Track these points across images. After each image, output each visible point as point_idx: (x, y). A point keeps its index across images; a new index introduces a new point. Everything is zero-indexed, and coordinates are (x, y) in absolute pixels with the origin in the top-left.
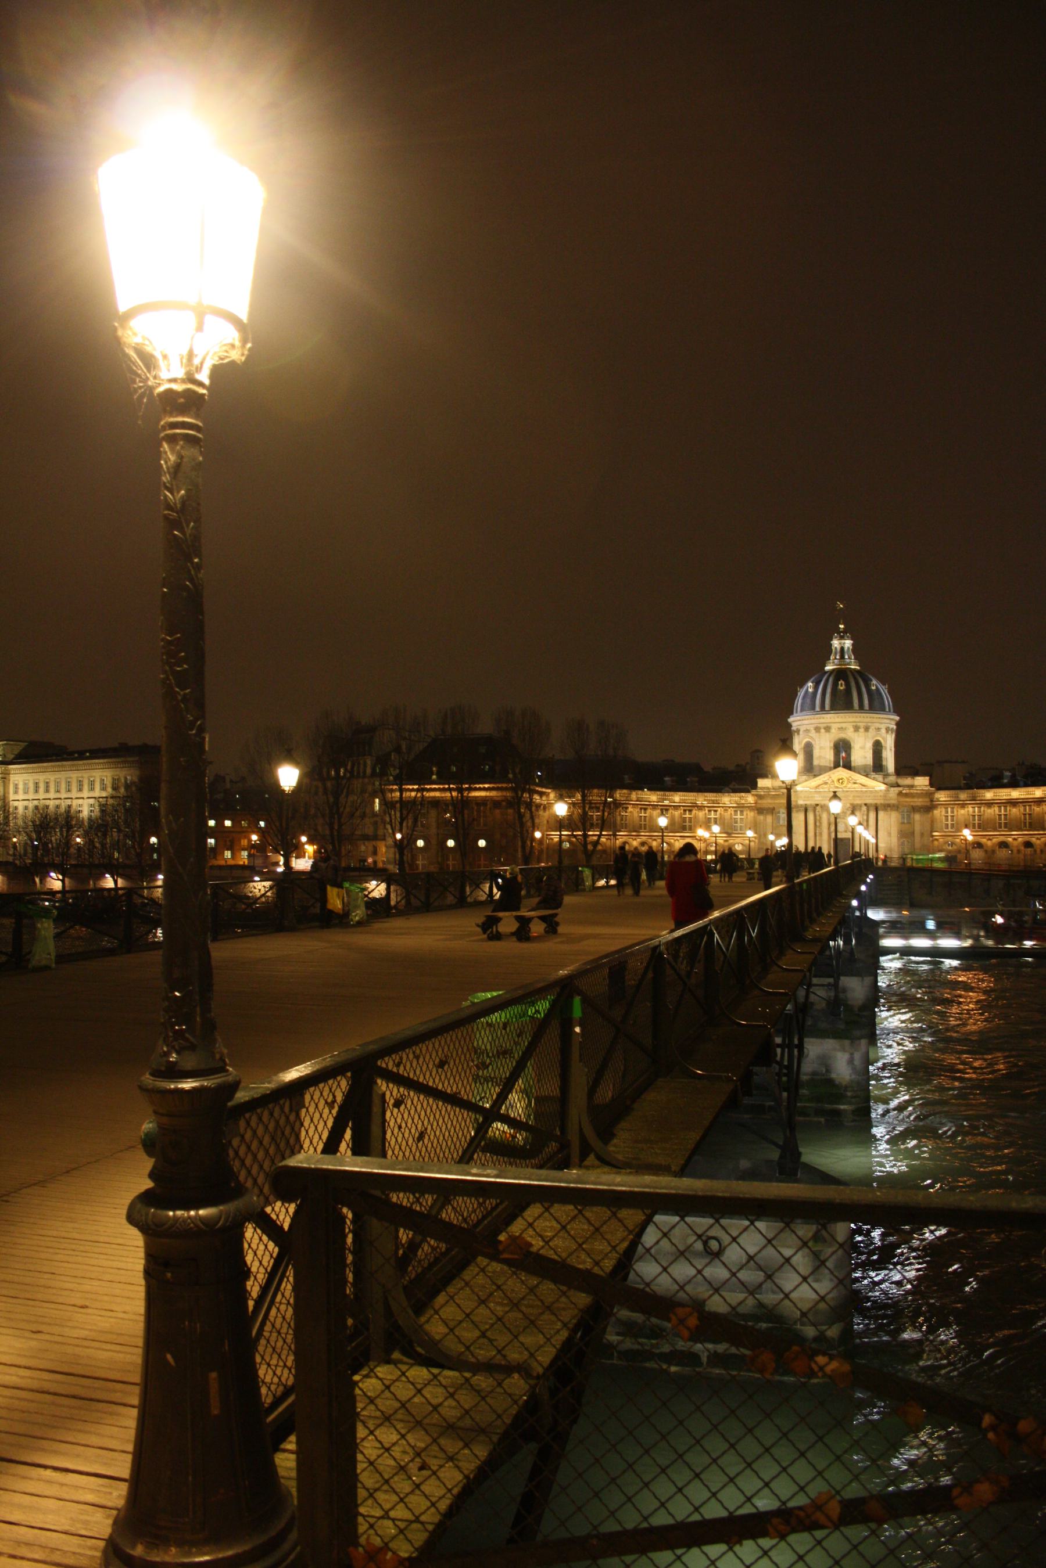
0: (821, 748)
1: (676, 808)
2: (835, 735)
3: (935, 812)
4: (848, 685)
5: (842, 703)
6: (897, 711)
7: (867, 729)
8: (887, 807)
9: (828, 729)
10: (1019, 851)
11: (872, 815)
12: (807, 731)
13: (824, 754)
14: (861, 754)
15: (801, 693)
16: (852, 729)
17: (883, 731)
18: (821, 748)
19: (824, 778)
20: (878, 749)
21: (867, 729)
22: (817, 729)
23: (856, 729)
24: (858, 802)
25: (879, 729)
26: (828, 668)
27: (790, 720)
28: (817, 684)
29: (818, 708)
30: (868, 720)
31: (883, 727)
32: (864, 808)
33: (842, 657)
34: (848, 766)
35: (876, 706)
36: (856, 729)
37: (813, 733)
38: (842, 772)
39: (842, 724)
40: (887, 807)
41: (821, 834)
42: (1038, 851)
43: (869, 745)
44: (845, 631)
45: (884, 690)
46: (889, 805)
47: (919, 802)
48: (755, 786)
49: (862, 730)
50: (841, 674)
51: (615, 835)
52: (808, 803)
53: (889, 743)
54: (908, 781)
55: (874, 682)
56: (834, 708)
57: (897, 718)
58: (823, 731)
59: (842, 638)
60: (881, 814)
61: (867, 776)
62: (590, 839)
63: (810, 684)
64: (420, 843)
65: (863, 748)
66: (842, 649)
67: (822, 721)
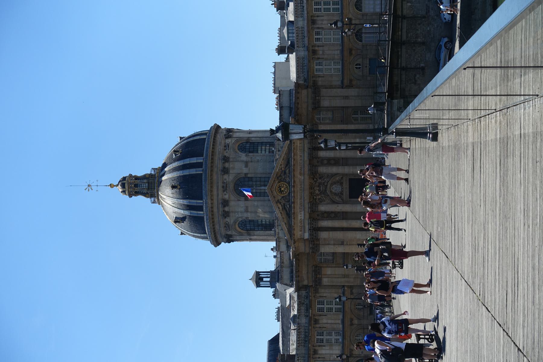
0: (247, 211)
3: (320, 83)
7: (226, 159)
9: (225, 203)
16: (226, 176)
17: (228, 141)
18: (247, 211)
22: (226, 214)
23: (225, 171)
25: (226, 146)
30: (216, 158)
36: (225, 171)
37: (230, 220)
43: (243, 157)
52: (307, 227)
58: (226, 209)
65: (246, 164)
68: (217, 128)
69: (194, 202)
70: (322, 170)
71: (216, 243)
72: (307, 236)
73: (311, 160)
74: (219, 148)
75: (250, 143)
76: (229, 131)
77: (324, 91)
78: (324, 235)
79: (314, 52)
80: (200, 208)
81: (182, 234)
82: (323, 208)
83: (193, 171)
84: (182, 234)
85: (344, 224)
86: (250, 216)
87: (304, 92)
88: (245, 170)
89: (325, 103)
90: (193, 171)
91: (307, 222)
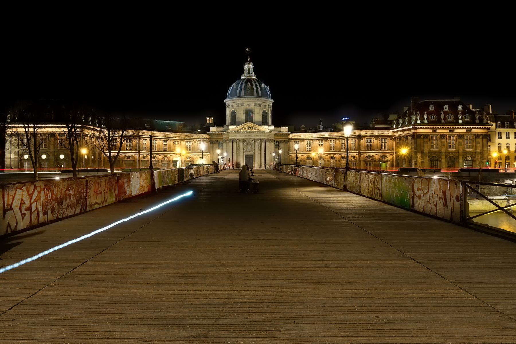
1: (171, 140)
4: (252, 85)
5: (249, 93)
6: (272, 98)
8: (270, 140)
10: (328, 161)
11: (263, 144)
12: (233, 106)
13: (241, 116)
14: (258, 117)
15: (230, 89)
16: (253, 105)
17: (267, 106)
19: (241, 126)
20: (265, 114)
21: (260, 105)
24: (257, 138)
25: (265, 106)
26: (242, 78)
27: (225, 101)
28: (238, 84)
29: (238, 95)
31: (267, 104)
32: (259, 141)
33: (249, 73)
34: (252, 121)
35: (264, 95)
38: (249, 124)
39: (249, 102)
40: (270, 140)
41: (239, 153)
42: (337, 161)
43: (261, 113)
44: (250, 61)
45: (267, 88)
46: (270, 140)
47: (283, 138)
48: (209, 130)
49: (258, 105)
50: (248, 80)
51: (139, 153)
53: (270, 111)
54: (278, 129)
55: (263, 84)
56: (246, 95)
57: (273, 101)
59: (249, 64)
60: (267, 144)
61: (261, 126)
62: (112, 154)
63: (234, 84)
64: (44, 157)
66: (249, 69)
67: (240, 101)
70: (257, 144)
72: (230, 138)
78: (231, 144)
82: (241, 144)
88: (256, 113)
91: (236, 138)
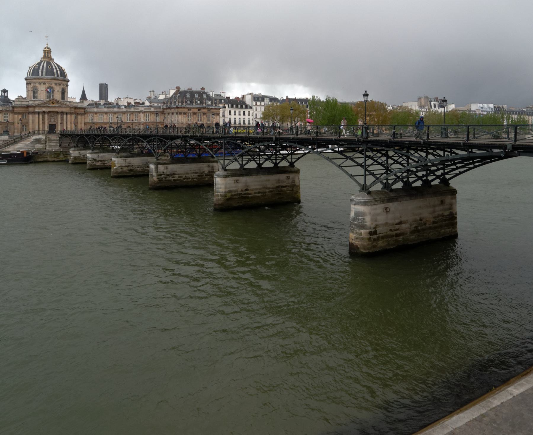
2: (47, 85)
9: (44, 84)
11: (65, 116)
22: (40, 83)
36: (56, 84)
37: (37, 85)
43: (60, 90)
60: (69, 116)
68: (68, 81)
69: (44, 73)
71: (26, 79)
73: (62, 112)
74: (63, 82)
75: (64, 92)
76: (67, 86)
77: (83, 116)
79: (96, 114)
80: (42, 74)
81: (30, 67)
83: (55, 73)
84: (30, 67)
85: (41, 122)
86: (39, 92)
87: (83, 111)
88: (56, 91)
89: (79, 117)
90: (55, 73)
